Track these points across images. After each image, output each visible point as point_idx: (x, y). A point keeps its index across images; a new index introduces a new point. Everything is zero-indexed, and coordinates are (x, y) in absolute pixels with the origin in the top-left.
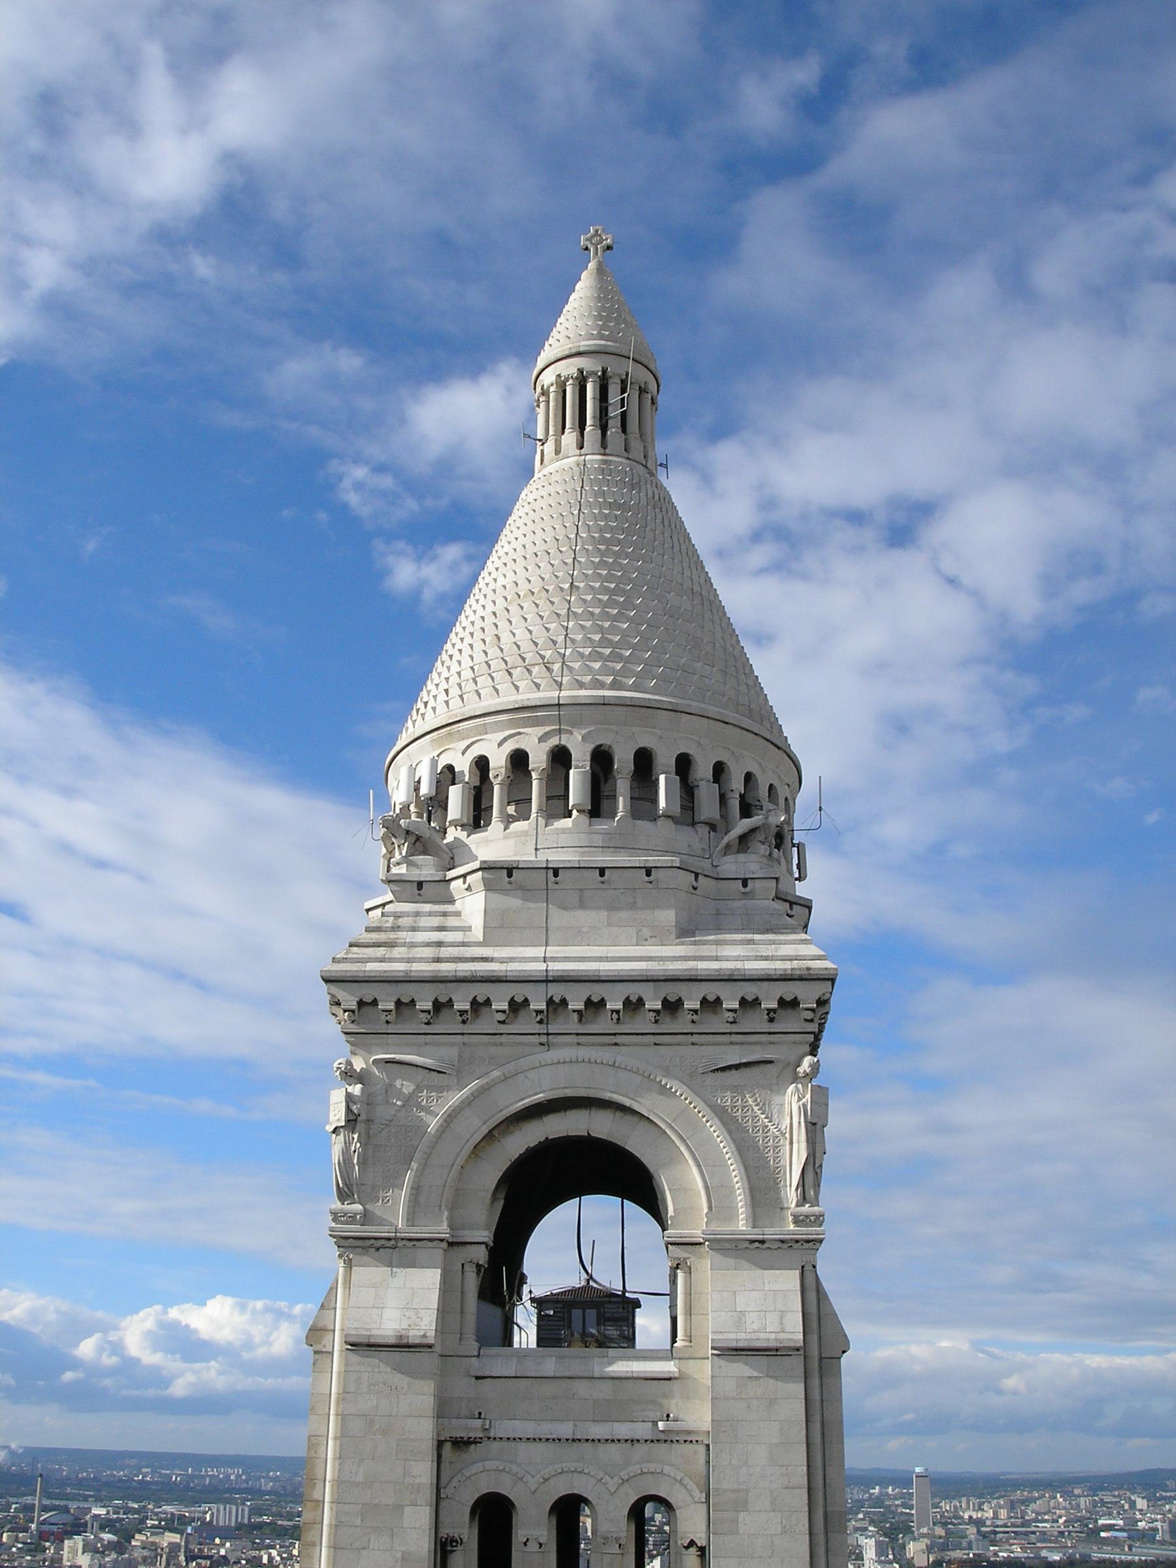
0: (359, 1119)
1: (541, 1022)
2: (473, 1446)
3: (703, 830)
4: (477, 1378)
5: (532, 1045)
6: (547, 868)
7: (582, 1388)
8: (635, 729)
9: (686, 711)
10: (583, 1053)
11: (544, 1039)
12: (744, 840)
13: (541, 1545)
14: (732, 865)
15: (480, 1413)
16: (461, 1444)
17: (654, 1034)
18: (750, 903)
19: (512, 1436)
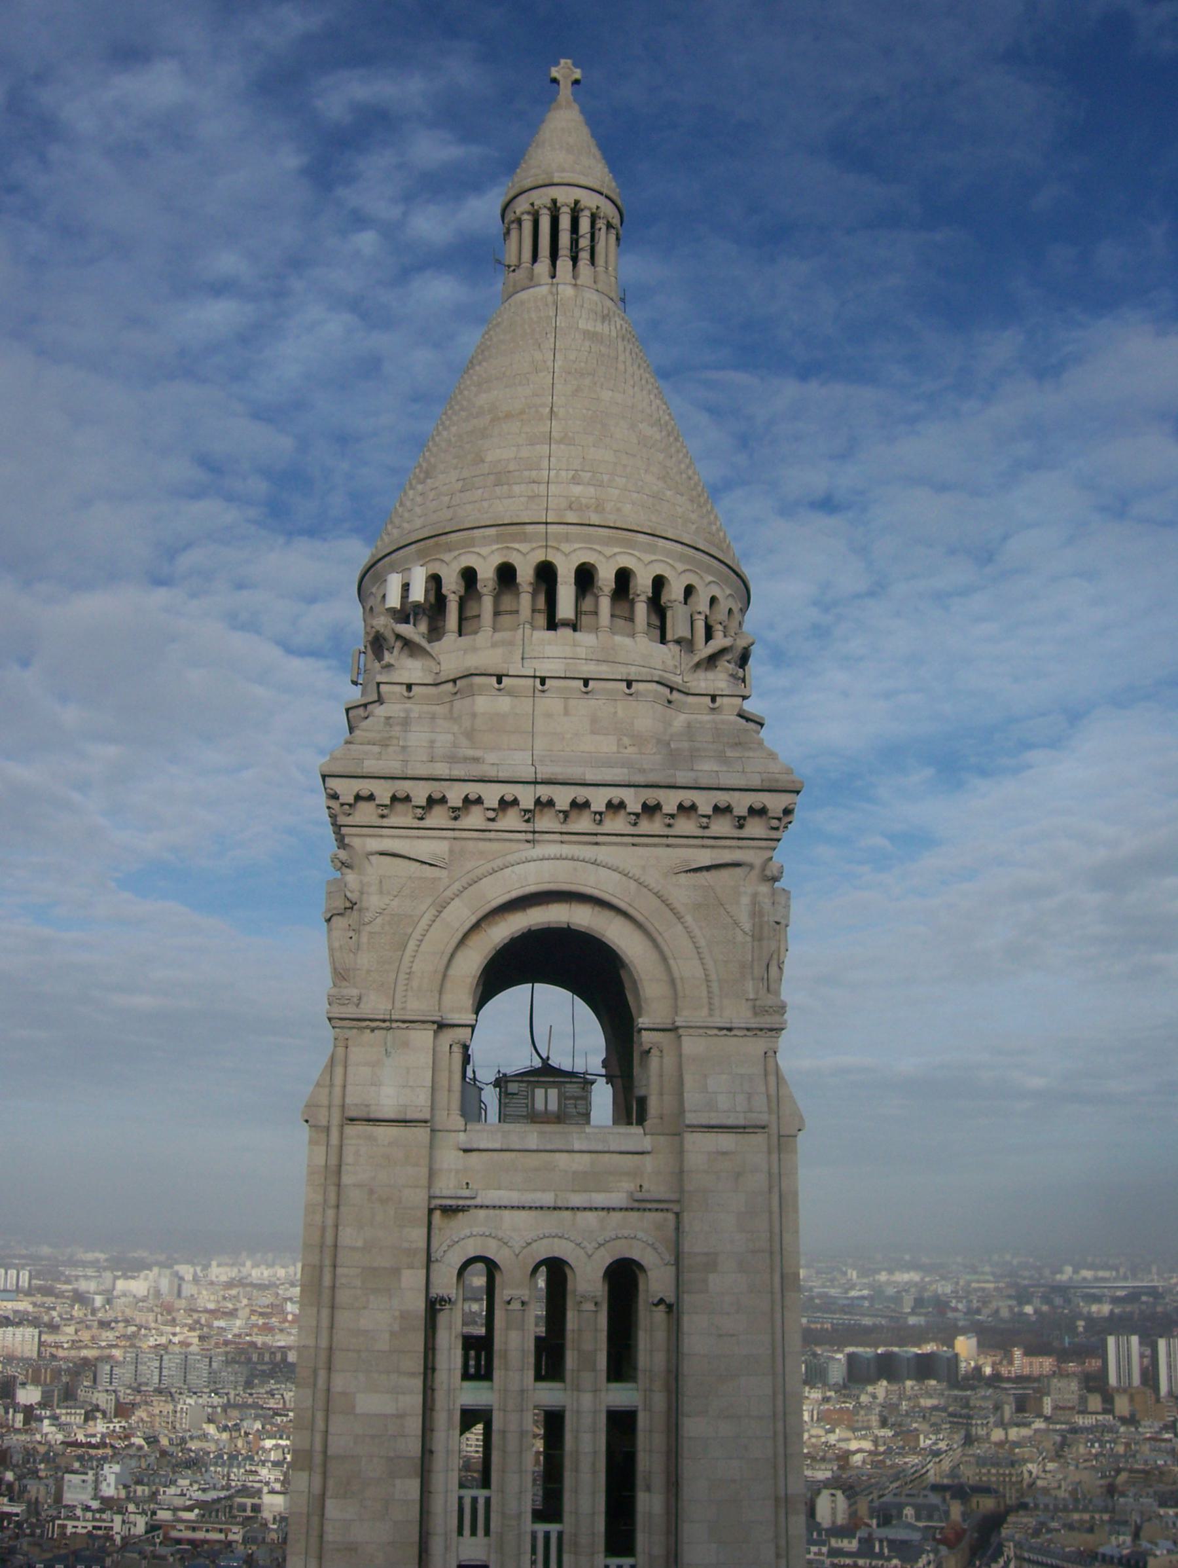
0: (355, 907)
1: (527, 821)
2: (461, 1214)
3: (675, 648)
4: (466, 1151)
5: (519, 841)
6: (535, 677)
7: (562, 1159)
8: (617, 550)
9: (664, 535)
10: (566, 850)
11: (530, 836)
12: (712, 661)
13: (523, 1303)
14: (707, 681)
15: (467, 1184)
16: (450, 1211)
17: (633, 835)
18: (718, 717)
19: (498, 1204)
